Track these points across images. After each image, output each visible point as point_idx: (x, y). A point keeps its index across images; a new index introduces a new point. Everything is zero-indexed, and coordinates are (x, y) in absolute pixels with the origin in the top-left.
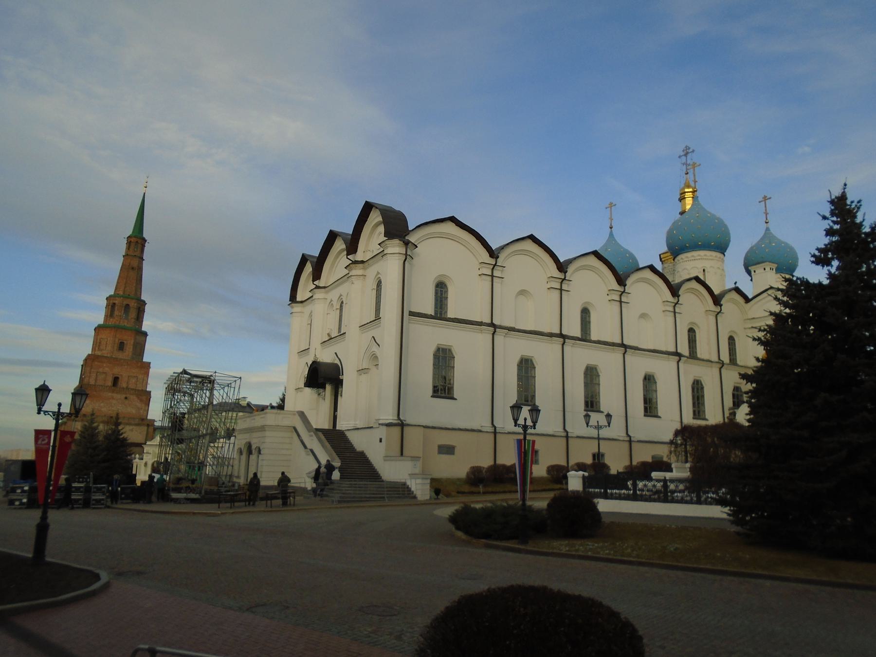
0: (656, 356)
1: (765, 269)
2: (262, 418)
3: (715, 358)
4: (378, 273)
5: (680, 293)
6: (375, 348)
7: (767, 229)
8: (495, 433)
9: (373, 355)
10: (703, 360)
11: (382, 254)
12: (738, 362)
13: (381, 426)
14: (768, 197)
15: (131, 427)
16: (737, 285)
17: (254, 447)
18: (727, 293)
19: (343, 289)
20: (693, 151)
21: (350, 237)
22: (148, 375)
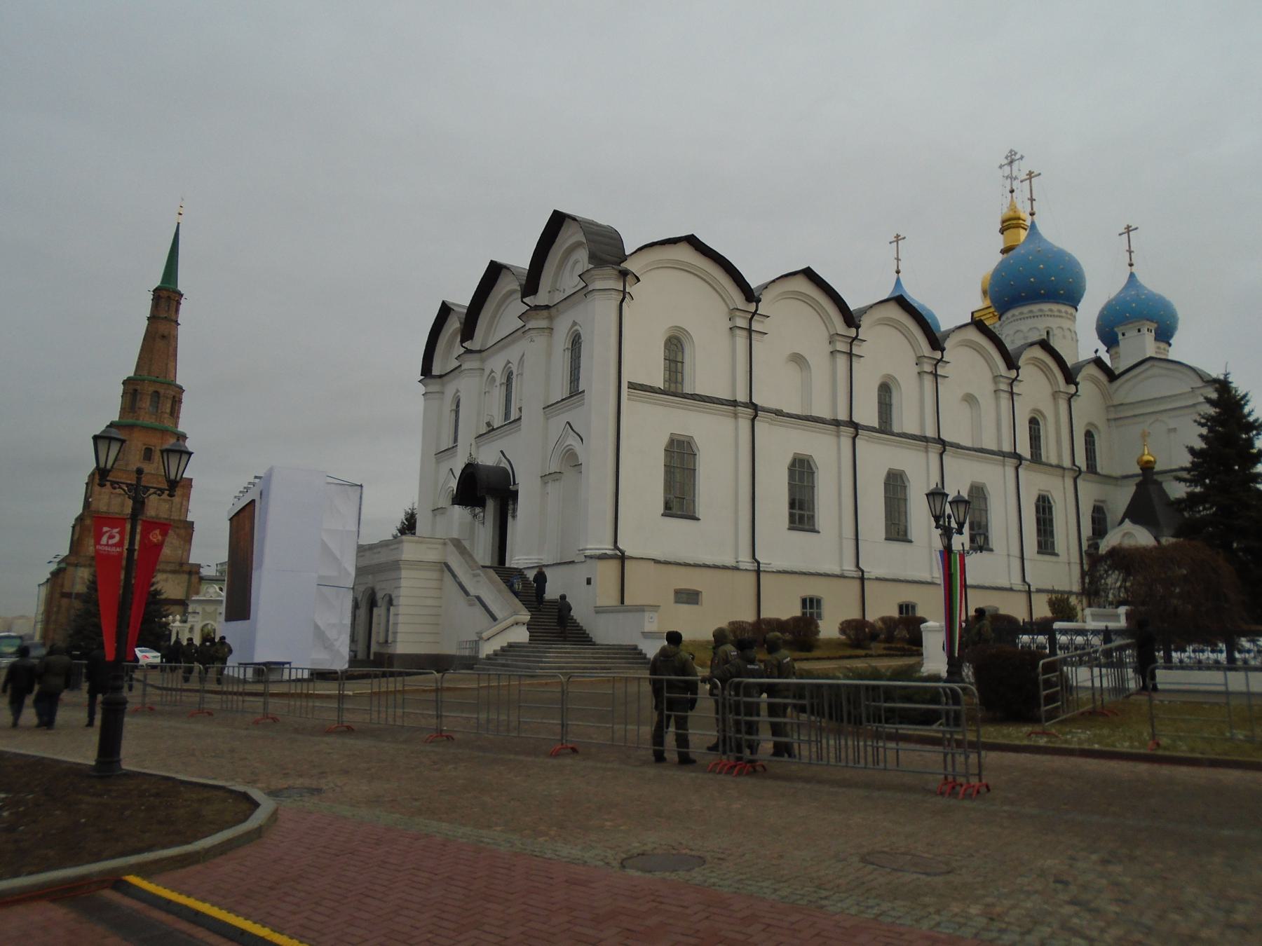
0: (986, 458)
1: (1139, 331)
2: (392, 550)
3: (1067, 463)
4: (575, 323)
5: (1019, 364)
6: (572, 441)
7: (1132, 275)
8: (758, 572)
9: (567, 452)
10: (1051, 466)
11: (584, 292)
12: (1099, 470)
13: (589, 561)
14: (1133, 227)
15: (165, 576)
16: (1098, 354)
17: (379, 595)
18: (1084, 366)
19: (512, 354)
20: (1022, 158)
21: (527, 272)
22: (189, 498)
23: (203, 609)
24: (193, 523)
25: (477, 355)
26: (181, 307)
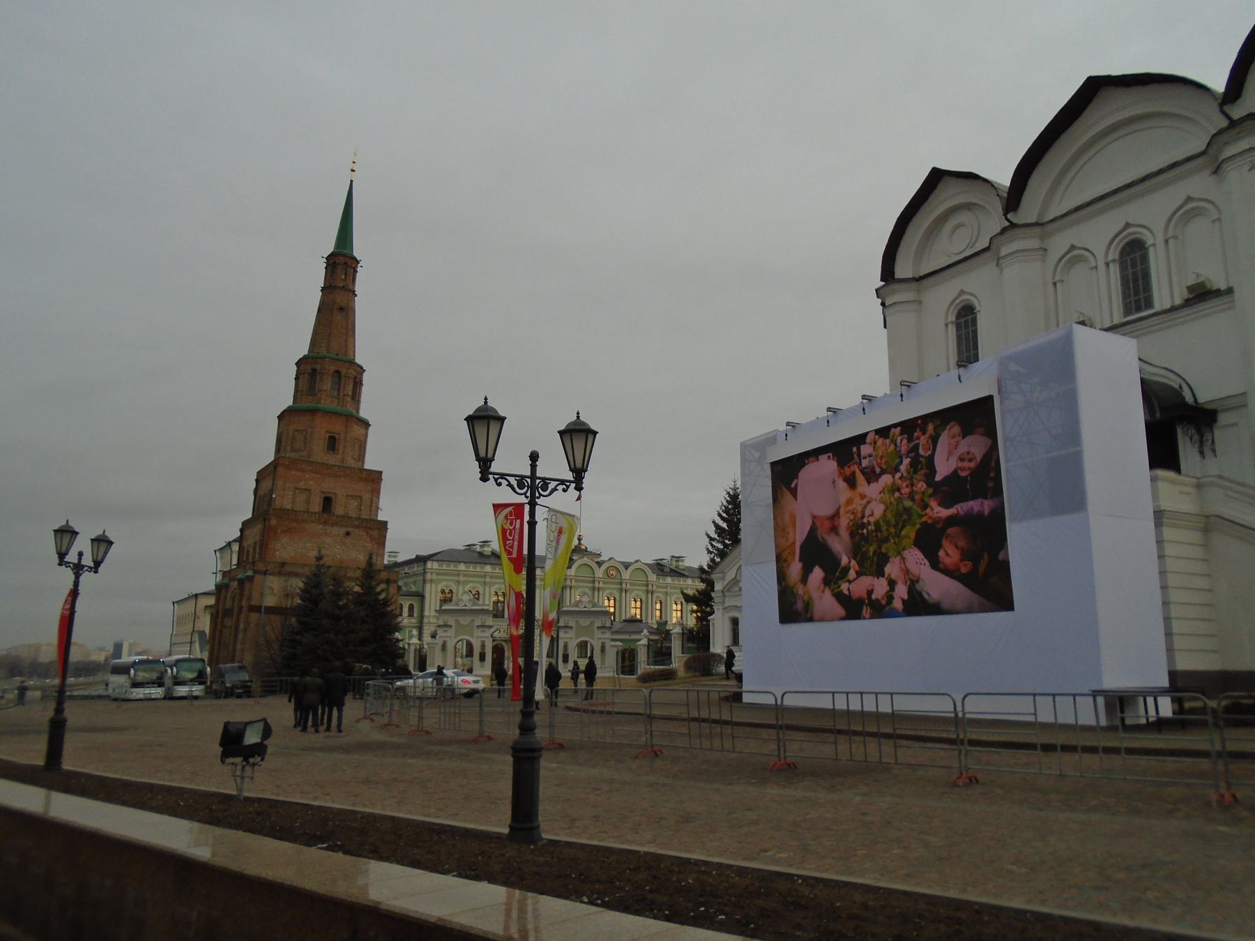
22: (379, 493)
23: (457, 621)
24: (386, 523)
25: (1037, 230)
26: (358, 275)
